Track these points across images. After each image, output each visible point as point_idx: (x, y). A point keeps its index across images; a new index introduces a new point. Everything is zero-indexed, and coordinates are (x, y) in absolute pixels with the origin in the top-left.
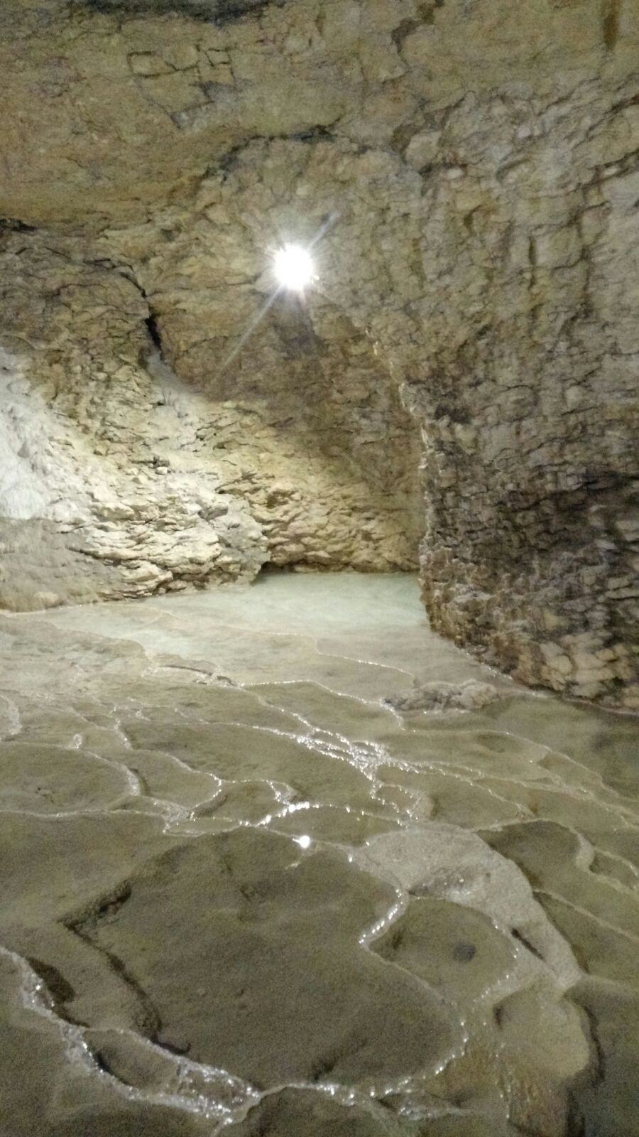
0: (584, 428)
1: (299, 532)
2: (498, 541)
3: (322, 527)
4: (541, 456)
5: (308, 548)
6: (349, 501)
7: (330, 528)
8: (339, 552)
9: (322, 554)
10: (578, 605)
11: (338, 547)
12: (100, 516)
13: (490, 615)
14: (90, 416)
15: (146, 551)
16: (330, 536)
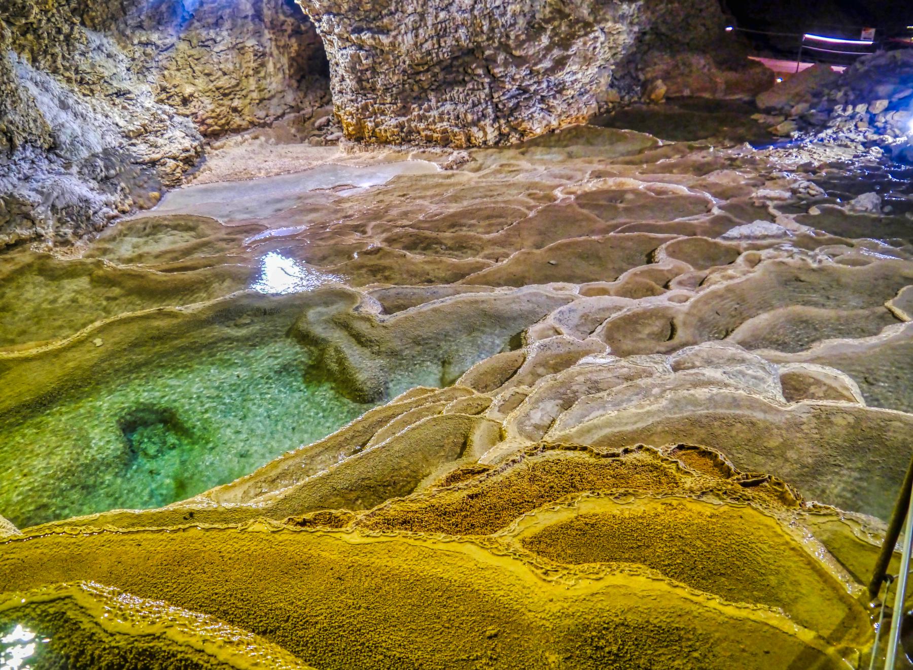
0: (445, 30)
1: (204, 117)
2: (404, 90)
3: (213, 111)
4: (427, 46)
5: (210, 126)
6: (221, 91)
7: (218, 110)
8: (223, 125)
9: (216, 128)
10: (480, 108)
11: (223, 121)
12: (127, 137)
13: (410, 126)
14: (67, 69)
15: (162, 152)
16: (219, 115)
